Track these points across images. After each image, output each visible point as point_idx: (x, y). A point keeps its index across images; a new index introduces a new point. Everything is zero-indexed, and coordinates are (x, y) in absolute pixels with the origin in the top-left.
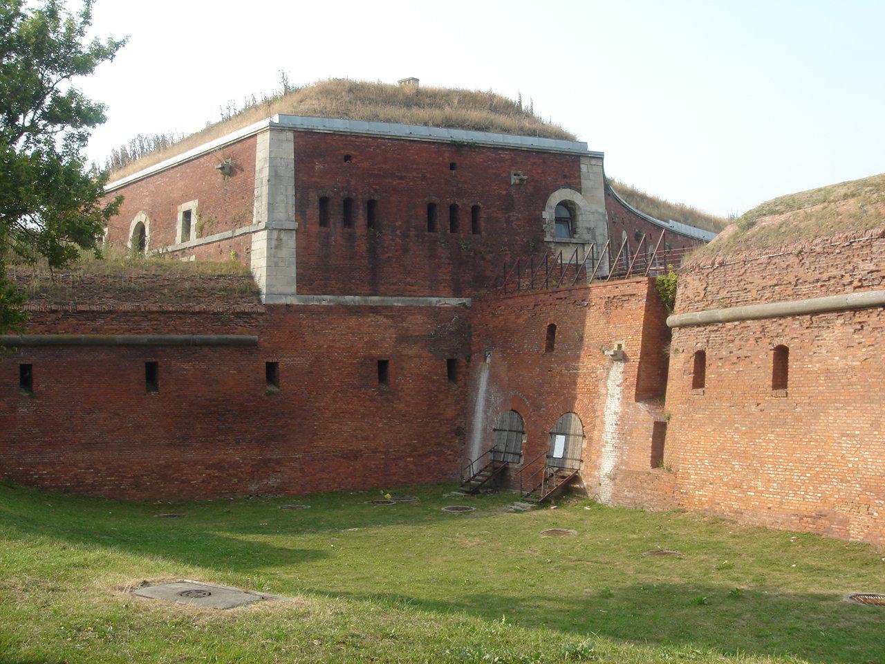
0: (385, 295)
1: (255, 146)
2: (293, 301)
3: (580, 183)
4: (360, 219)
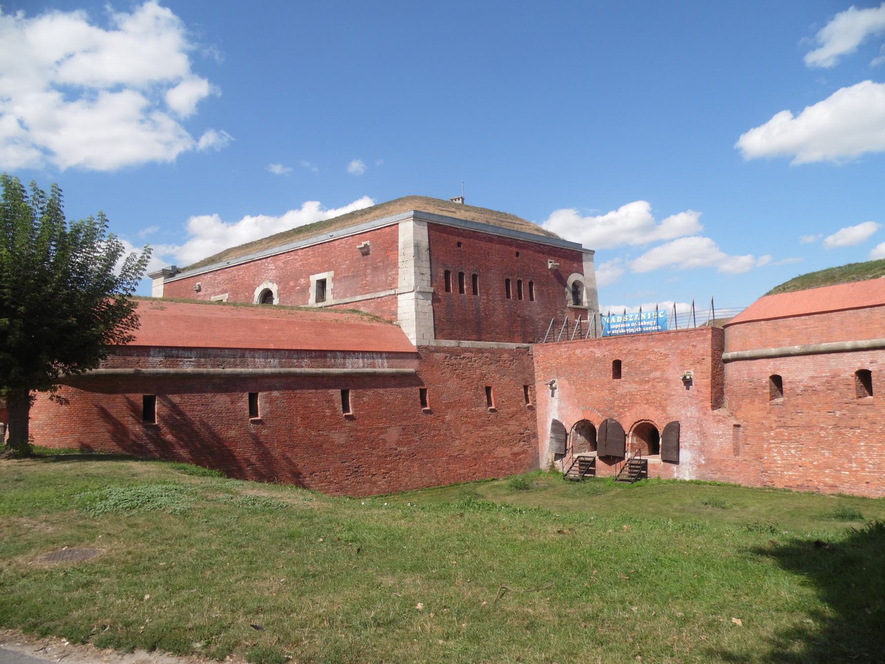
2: (433, 343)
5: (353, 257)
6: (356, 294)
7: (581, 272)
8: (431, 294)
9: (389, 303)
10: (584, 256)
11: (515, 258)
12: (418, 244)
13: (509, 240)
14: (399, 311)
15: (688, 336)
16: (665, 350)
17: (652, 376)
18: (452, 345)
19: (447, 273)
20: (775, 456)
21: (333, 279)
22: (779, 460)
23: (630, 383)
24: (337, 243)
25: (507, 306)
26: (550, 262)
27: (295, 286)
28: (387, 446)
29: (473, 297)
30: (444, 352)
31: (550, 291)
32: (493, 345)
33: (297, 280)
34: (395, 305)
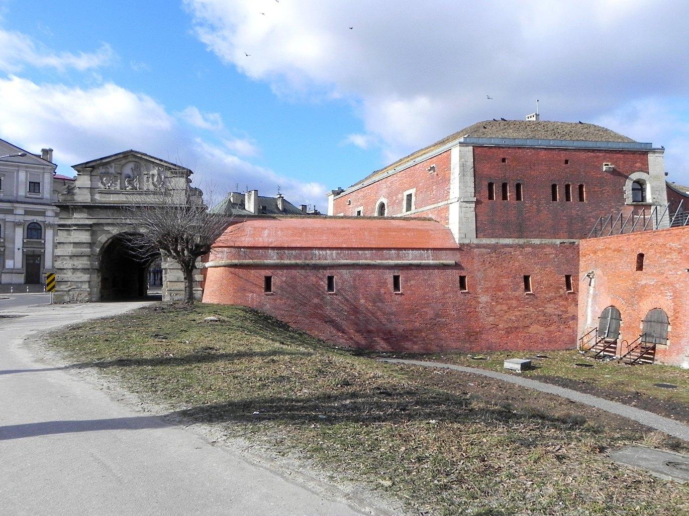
1: (450, 155)
2: (475, 241)
11: (564, 165)
19: (490, 185)
26: (606, 165)
27: (396, 200)
29: (515, 202)
32: (537, 241)
33: (397, 195)
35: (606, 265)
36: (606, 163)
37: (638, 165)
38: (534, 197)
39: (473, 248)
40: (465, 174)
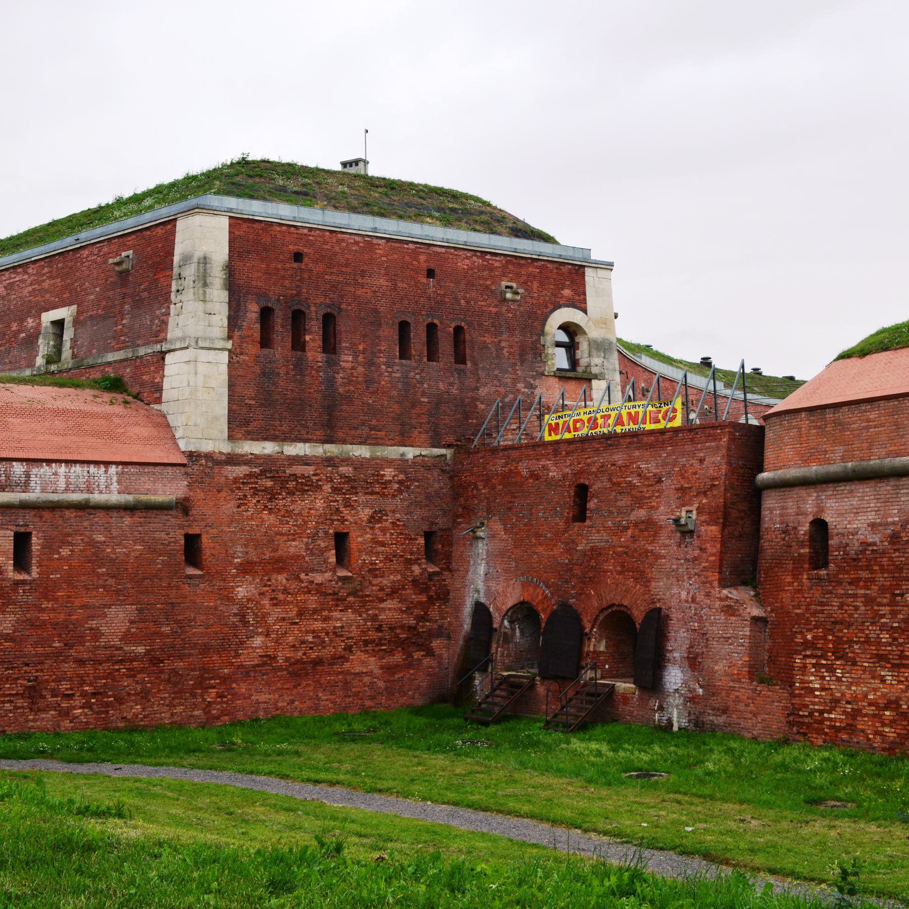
0: (344, 442)
3: (584, 301)
4: (313, 338)
5: (107, 280)
6: (108, 349)
7: (582, 305)
8: (227, 353)
9: (152, 368)
10: (590, 275)
12: (205, 258)
13: (411, 246)
14: (166, 385)
15: (692, 440)
16: (657, 467)
17: (632, 517)
18: (266, 452)
19: (266, 314)
20: (811, 682)
21: (76, 322)
22: (817, 689)
23: (598, 532)
24: (86, 253)
25: (398, 375)
28: (103, 641)
30: (247, 462)
31: (503, 344)
34: (161, 372)
35: (510, 509)
36: (509, 284)
37: (567, 292)
38: (361, 347)
39: (219, 463)
40: (208, 282)
